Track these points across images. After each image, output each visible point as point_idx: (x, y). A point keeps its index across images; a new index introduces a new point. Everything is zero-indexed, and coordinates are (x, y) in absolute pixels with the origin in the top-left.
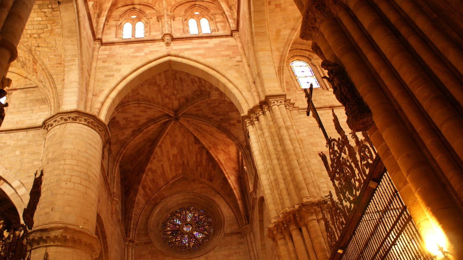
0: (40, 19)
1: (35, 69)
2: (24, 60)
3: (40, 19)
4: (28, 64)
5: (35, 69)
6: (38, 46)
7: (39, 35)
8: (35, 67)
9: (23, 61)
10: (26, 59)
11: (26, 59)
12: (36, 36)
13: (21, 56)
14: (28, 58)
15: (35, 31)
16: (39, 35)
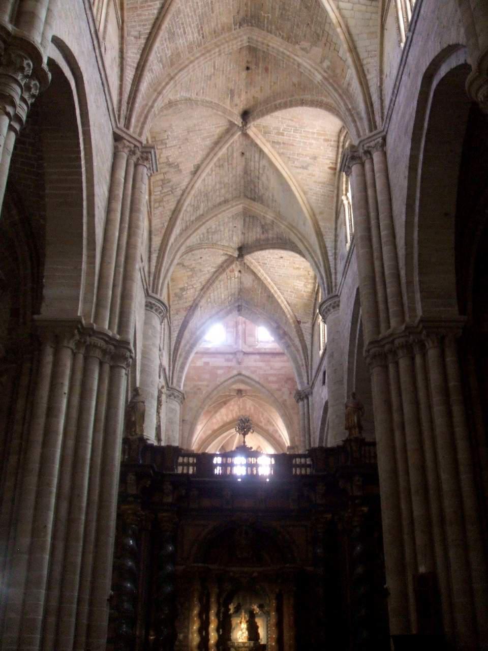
0: (223, 297)
1: (179, 311)
2: (185, 296)
3: (223, 297)
4: (181, 302)
5: (179, 311)
6: (201, 307)
7: (210, 302)
8: (181, 310)
9: (182, 295)
10: (186, 299)
11: (186, 299)
12: (209, 300)
13: (188, 293)
14: (187, 300)
15: (212, 297)
16: (210, 302)
